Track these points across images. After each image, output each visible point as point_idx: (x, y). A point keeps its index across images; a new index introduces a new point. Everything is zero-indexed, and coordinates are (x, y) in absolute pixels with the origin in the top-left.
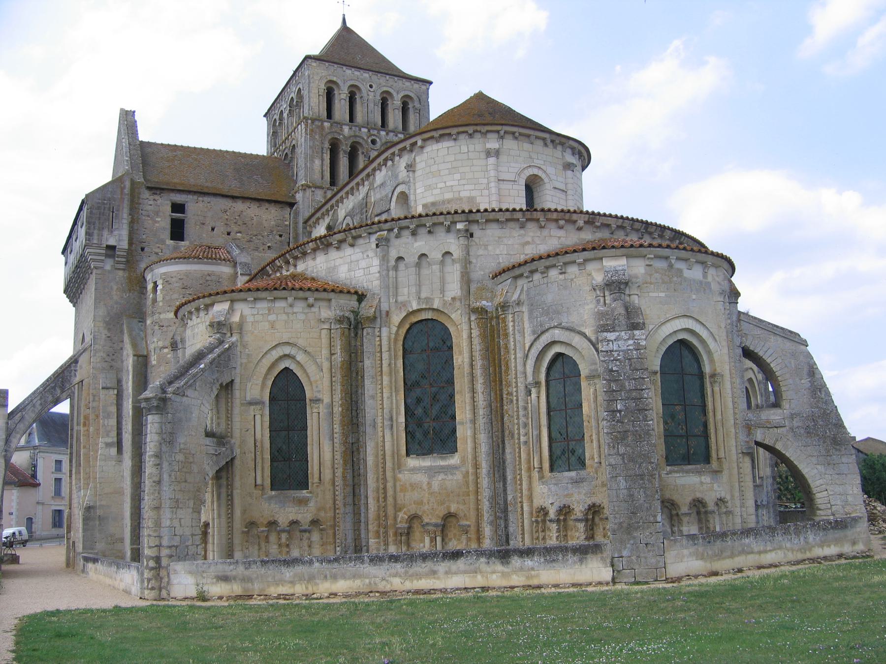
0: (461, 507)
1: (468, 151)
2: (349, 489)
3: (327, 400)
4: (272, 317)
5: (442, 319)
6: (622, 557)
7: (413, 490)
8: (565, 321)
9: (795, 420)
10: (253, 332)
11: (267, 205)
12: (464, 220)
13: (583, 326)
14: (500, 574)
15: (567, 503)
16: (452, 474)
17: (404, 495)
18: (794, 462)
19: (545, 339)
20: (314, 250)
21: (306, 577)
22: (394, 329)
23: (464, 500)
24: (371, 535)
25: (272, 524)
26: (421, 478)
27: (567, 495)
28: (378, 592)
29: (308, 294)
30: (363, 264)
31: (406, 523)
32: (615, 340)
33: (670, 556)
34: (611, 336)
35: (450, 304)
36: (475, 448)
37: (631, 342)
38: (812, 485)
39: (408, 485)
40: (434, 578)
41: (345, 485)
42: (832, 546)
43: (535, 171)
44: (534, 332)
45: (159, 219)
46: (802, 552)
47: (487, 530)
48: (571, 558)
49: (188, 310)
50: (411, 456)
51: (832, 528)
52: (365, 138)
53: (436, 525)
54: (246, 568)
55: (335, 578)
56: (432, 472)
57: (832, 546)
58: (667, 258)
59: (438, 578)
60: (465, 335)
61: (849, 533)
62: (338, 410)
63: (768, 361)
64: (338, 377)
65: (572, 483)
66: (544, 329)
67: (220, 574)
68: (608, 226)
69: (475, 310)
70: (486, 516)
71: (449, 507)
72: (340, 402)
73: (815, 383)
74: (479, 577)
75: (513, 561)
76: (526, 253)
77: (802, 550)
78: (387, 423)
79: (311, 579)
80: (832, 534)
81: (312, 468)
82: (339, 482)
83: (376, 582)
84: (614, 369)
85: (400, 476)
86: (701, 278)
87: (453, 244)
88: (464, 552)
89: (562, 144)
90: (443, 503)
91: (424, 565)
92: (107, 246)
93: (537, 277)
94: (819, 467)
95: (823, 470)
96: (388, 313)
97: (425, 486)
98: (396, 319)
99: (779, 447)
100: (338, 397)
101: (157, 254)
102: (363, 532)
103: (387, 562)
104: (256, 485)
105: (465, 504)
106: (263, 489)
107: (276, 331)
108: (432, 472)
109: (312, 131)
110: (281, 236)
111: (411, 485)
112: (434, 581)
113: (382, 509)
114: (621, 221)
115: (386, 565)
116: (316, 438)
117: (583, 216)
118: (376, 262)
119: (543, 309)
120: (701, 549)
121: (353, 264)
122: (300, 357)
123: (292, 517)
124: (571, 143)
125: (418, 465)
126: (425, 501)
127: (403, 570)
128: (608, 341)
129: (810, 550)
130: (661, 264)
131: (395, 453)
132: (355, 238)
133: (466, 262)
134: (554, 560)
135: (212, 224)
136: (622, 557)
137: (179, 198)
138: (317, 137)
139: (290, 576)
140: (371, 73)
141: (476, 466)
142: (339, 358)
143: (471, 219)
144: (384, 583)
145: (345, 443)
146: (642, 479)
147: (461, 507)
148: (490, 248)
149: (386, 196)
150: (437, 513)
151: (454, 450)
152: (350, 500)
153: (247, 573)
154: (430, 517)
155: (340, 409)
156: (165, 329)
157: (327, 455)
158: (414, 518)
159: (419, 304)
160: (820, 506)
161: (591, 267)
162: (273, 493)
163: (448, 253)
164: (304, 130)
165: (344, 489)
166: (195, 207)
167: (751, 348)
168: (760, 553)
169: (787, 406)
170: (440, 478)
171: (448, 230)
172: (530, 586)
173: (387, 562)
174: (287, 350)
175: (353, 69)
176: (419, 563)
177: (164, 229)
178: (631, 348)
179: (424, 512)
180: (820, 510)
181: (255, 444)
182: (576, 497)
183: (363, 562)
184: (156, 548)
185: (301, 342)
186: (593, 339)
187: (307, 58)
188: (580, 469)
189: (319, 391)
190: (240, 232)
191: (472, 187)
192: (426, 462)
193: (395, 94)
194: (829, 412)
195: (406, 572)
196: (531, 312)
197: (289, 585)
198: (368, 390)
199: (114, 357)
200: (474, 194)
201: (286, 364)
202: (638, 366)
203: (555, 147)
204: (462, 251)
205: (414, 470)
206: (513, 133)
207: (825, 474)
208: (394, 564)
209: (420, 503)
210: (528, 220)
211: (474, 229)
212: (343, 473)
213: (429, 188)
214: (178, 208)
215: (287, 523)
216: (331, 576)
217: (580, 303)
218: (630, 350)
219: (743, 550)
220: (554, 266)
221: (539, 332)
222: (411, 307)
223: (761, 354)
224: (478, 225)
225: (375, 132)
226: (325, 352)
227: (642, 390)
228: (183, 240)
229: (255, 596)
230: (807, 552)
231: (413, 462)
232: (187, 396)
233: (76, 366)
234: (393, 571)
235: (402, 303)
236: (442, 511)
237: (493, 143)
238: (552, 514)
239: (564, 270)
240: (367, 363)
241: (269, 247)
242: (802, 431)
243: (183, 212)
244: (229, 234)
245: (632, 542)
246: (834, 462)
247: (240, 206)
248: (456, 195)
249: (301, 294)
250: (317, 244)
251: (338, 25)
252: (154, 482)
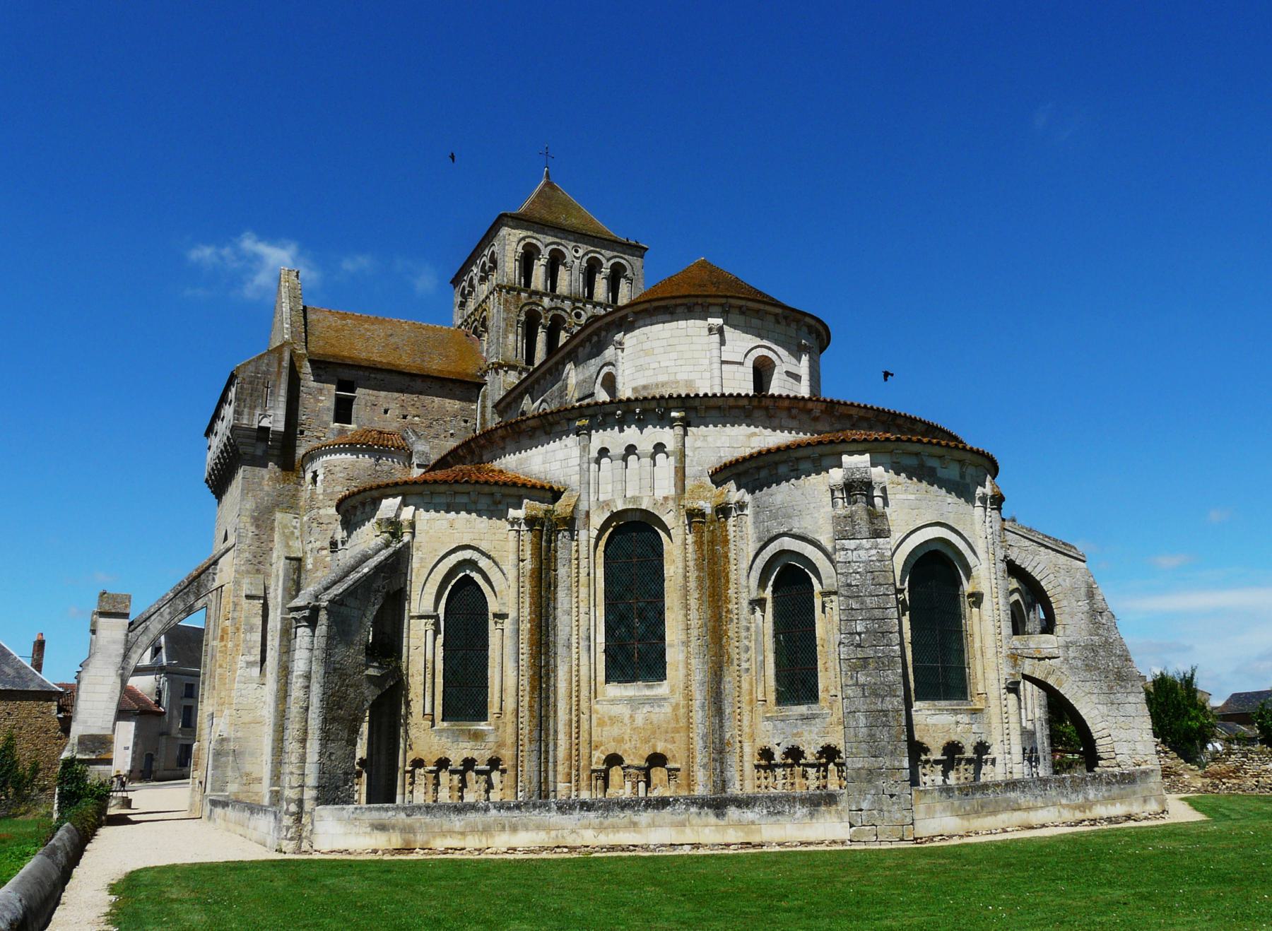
0: (670, 746)
1: (687, 327)
2: (536, 721)
3: (513, 615)
6: (861, 810)
7: (612, 724)
9: (1071, 649)
10: (428, 532)
11: (451, 385)
12: (679, 405)
13: (817, 532)
14: (713, 828)
15: (796, 744)
16: (659, 706)
17: (602, 731)
18: (1071, 701)
20: (503, 438)
21: (480, 828)
22: (594, 533)
23: (673, 737)
24: (560, 778)
26: (623, 710)
27: (795, 735)
28: (566, 847)
29: (495, 489)
31: (603, 764)
32: (855, 549)
33: (920, 808)
34: (851, 544)
35: (662, 504)
37: (874, 552)
38: (1092, 729)
39: (606, 719)
40: (635, 831)
41: (532, 716)
42: (1118, 805)
44: (759, 539)
45: (323, 398)
46: (1081, 811)
47: (700, 775)
48: (801, 811)
49: (352, 504)
50: (612, 684)
51: (1117, 782)
52: (569, 310)
53: (639, 768)
54: (408, 815)
55: (514, 829)
56: (633, 702)
57: (1118, 805)
58: (917, 454)
59: (640, 832)
61: (1138, 787)
62: (526, 626)
63: (1038, 578)
65: (802, 719)
66: (771, 535)
67: (376, 822)
68: (850, 416)
70: (700, 758)
71: (654, 746)
72: (529, 618)
73: (1095, 606)
74: (688, 830)
75: (730, 812)
76: (752, 446)
77: (1081, 808)
78: (583, 644)
79: (486, 830)
80: (1116, 789)
81: (493, 695)
82: (525, 713)
83: (565, 835)
84: (853, 583)
85: (596, 707)
86: (958, 478)
88: (671, 800)
89: (798, 321)
90: (647, 741)
91: (622, 815)
92: (259, 427)
94: (1100, 707)
95: (1106, 712)
96: (588, 514)
97: (627, 720)
98: (597, 520)
99: (1051, 681)
100: (526, 611)
101: (319, 438)
102: (551, 773)
103: (578, 810)
104: (424, 715)
105: (675, 743)
106: (433, 721)
107: (455, 531)
109: (506, 301)
110: (466, 421)
111: (610, 718)
112: (635, 835)
113: (574, 748)
114: (864, 411)
115: (576, 814)
116: (498, 660)
117: (819, 404)
119: (771, 511)
120: (957, 803)
121: (548, 454)
122: (483, 563)
123: (467, 754)
124: (808, 319)
125: (619, 695)
126: (627, 738)
127: (597, 821)
128: (847, 550)
129: (1090, 810)
131: (592, 679)
132: (551, 425)
134: (779, 812)
135: (386, 406)
136: (861, 810)
138: (512, 308)
139: (460, 827)
140: (576, 235)
142: (528, 565)
143: (688, 405)
144: (574, 835)
145: (533, 666)
146: (886, 716)
147: (670, 746)
148: (709, 439)
149: (590, 377)
150: (641, 752)
151: (662, 676)
152: (536, 734)
153: (409, 821)
154: (632, 757)
155: (529, 625)
156: (324, 526)
158: (614, 760)
159: (625, 503)
160: (1102, 755)
162: (445, 724)
164: (497, 300)
165: (530, 721)
167: (1018, 562)
168: (1029, 809)
169: (1061, 633)
170: (645, 710)
172: (750, 843)
173: (578, 810)
174: (467, 554)
175: (556, 231)
176: (617, 812)
177: (329, 409)
178: (874, 558)
179: (625, 751)
180: (1102, 759)
181: (425, 664)
182: (806, 736)
183: (549, 811)
184: (299, 789)
185: (484, 546)
186: (829, 548)
187: (502, 216)
188: (812, 703)
189: (504, 604)
190: (418, 416)
191: (691, 368)
193: (604, 261)
194: (1111, 640)
195: (601, 823)
196: (756, 514)
197: (460, 837)
198: (562, 604)
199: (261, 559)
200: (692, 376)
202: (882, 580)
203: (788, 325)
204: (677, 443)
205: (613, 701)
206: (740, 308)
207: (1108, 716)
208: (586, 813)
209: (620, 740)
210: (754, 408)
212: (530, 701)
213: (640, 368)
215: (460, 761)
216: (510, 827)
217: (815, 505)
218: (873, 561)
219: (1008, 805)
220: (785, 462)
221: (766, 539)
222: (616, 507)
223: (1029, 569)
224: (697, 412)
225: (580, 305)
226: (512, 558)
227: (886, 609)
228: (350, 424)
229: (417, 850)
230: (1087, 811)
231: (615, 690)
232: (346, 605)
233: (215, 569)
234: (585, 822)
235: (604, 502)
236: (647, 752)
239: (796, 467)
240: (562, 571)
241: (452, 434)
242: (1080, 663)
243: (354, 393)
244: (405, 417)
245: (873, 792)
246: (1119, 701)
248: (672, 378)
249: (486, 489)
250: (507, 430)
252: (301, 708)
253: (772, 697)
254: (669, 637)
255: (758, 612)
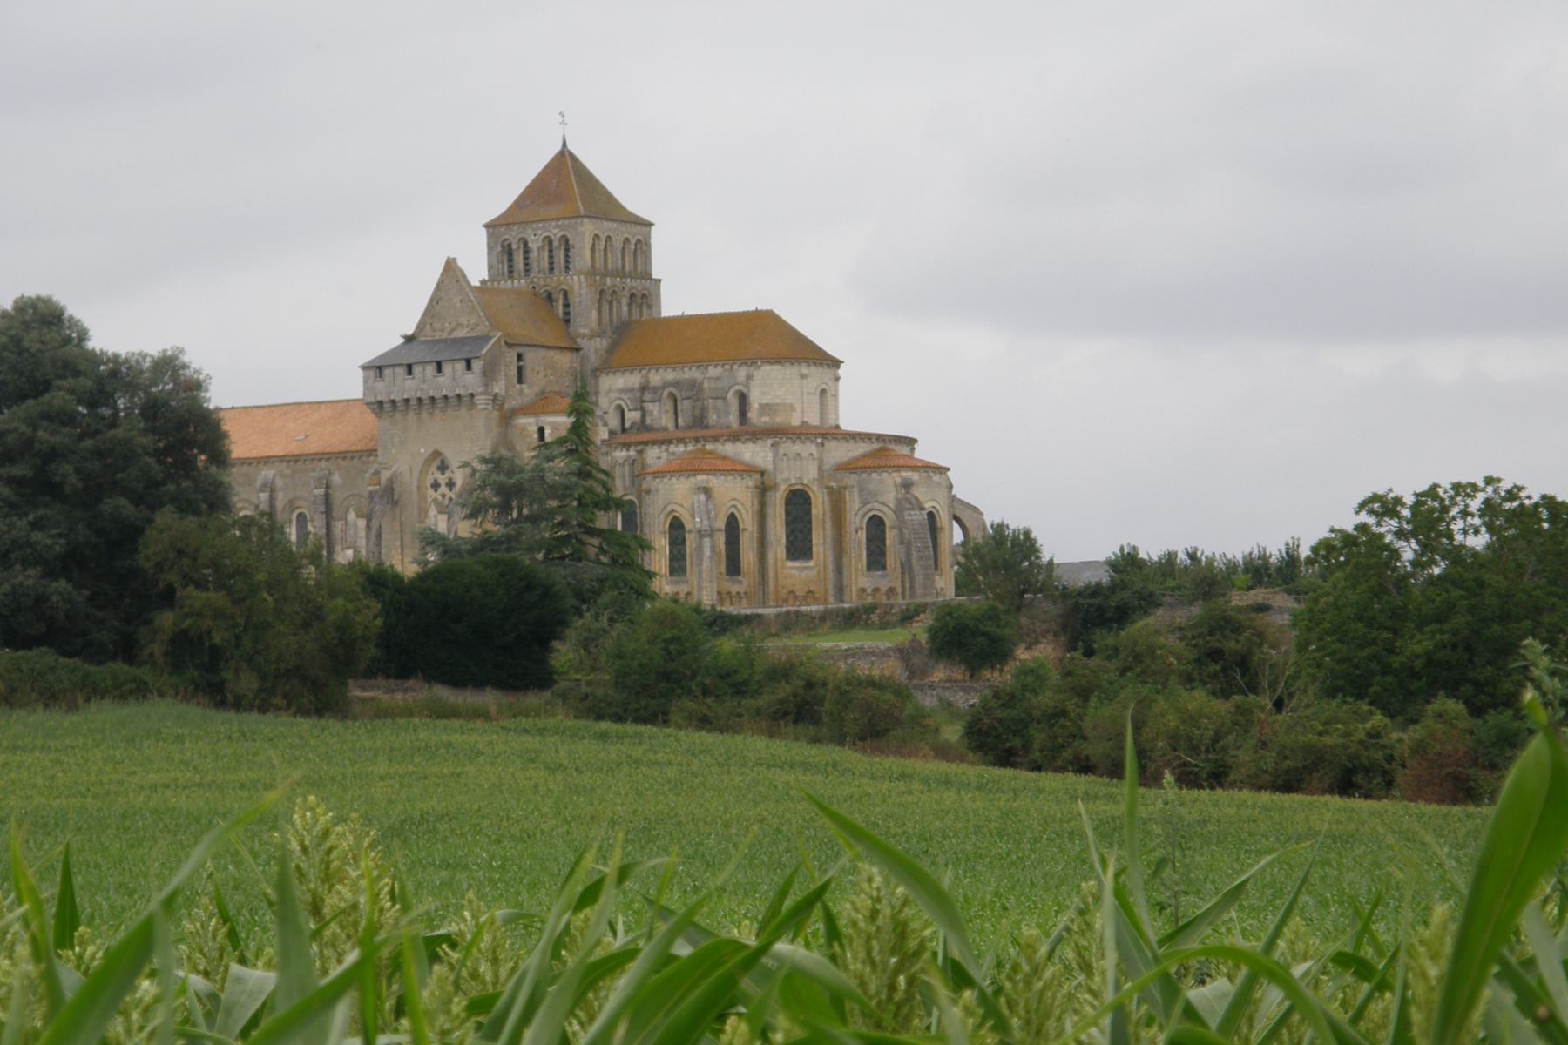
3: (751, 529)
4: (727, 485)
5: (808, 491)
8: (880, 499)
19: (868, 507)
25: (729, 593)
26: (794, 572)
30: (762, 454)
36: (825, 557)
43: (823, 386)
60: (821, 499)
64: (756, 518)
69: (828, 488)
82: (756, 573)
87: (813, 449)
93: (864, 475)
100: (755, 528)
108: (801, 569)
118: (770, 455)
122: (739, 506)
130: (925, 475)
133: (821, 461)
137: (521, 350)
141: (825, 567)
151: (810, 557)
157: (751, 559)
161: (895, 474)
163: (811, 454)
166: (531, 356)
171: (812, 442)
174: (734, 503)
192: (797, 564)
201: (733, 510)
205: (792, 568)
211: (825, 442)
214: (520, 357)
231: (790, 564)
236: (806, 590)
237: (805, 370)
238: (869, 591)
247: (551, 353)
251: (559, 147)
253: (865, 568)
254: (814, 542)
255: (859, 533)
